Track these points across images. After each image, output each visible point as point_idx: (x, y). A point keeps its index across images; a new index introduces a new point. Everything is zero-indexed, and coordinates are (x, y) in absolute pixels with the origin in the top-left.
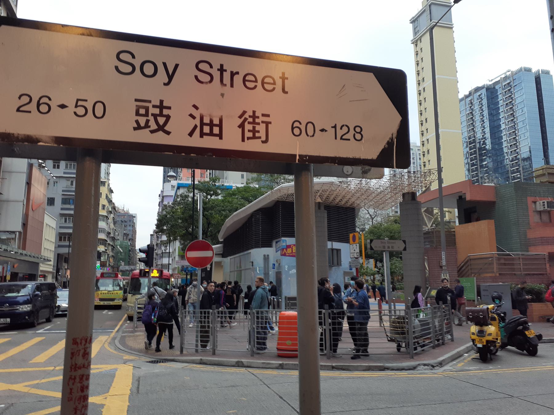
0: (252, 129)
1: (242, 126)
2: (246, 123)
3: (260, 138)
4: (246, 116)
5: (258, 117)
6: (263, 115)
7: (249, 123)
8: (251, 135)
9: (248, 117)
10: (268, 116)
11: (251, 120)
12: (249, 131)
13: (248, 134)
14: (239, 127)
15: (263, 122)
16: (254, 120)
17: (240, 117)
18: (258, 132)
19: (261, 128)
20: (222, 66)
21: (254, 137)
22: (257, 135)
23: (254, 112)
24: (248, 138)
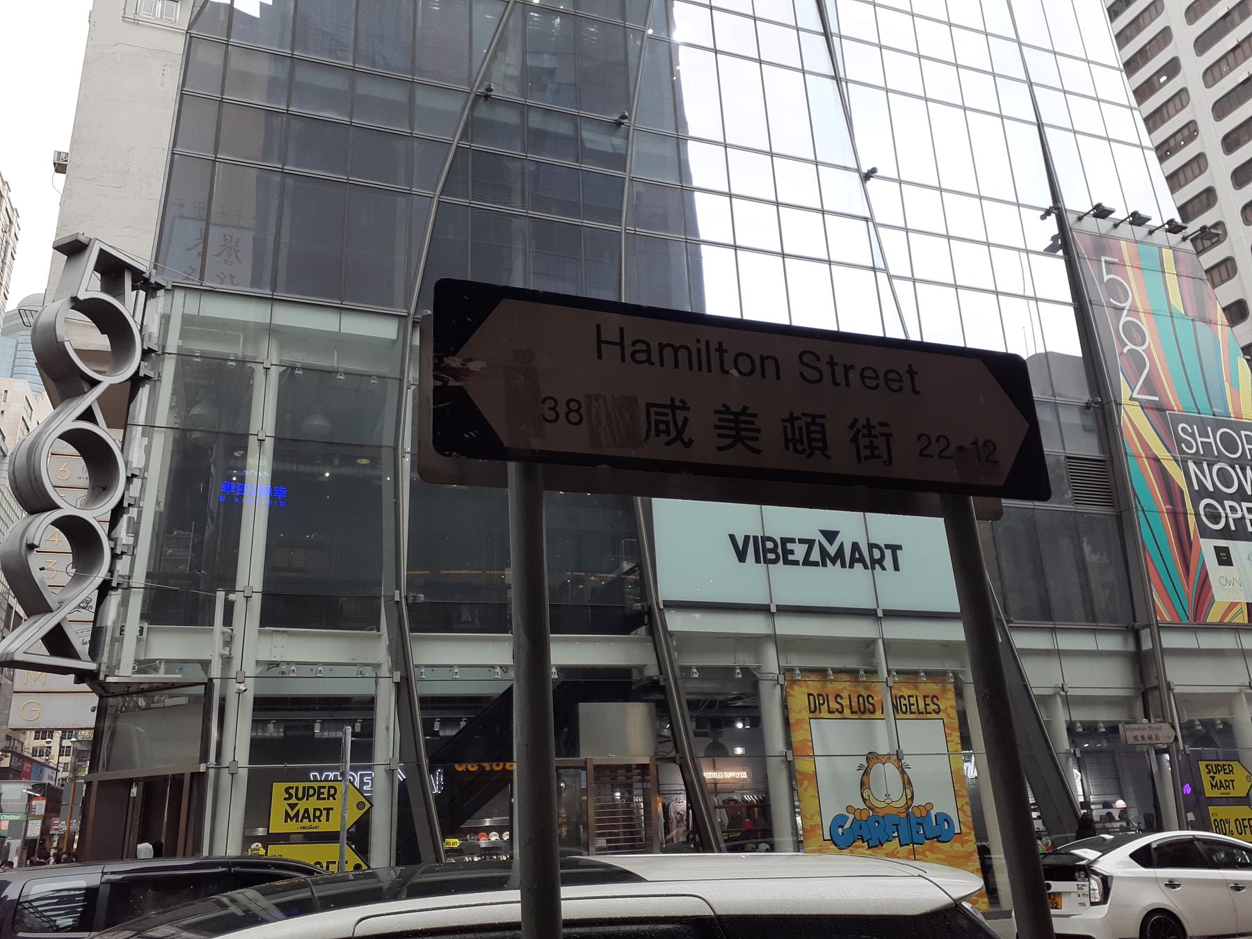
1: (854, 440)
3: (880, 457)
4: (859, 425)
8: (867, 452)
12: (866, 447)
14: (852, 441)
17: (851, 427)
19: (880, 442)
21: (873, 456)
22: (877, 453)
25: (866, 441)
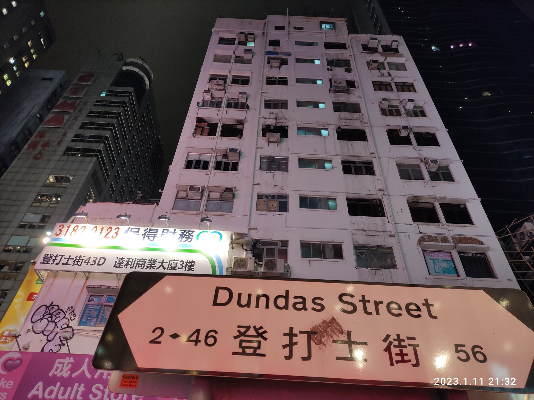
0: (399, 352)
1: (388, 349)
2: (392, 347)
3: (409, 361)
4: (391, 339)
5: (403, 340)
6: (408, 338)
7: (395, 346)
8: (399, 358)
9: (392, 341)
10: (414, 338)
11: (396, 343)
12: (397, 354)
13: (396, 358)
15: (409, 345)
16: (400, 343)
17: (385, 340)
18: (407, 355)
19: (409, 351)
20: (363, 297)
21: (403, 361)
22: (406, 358)
23: (398, 336)
24: (397, 362)
25: (397, 350)
